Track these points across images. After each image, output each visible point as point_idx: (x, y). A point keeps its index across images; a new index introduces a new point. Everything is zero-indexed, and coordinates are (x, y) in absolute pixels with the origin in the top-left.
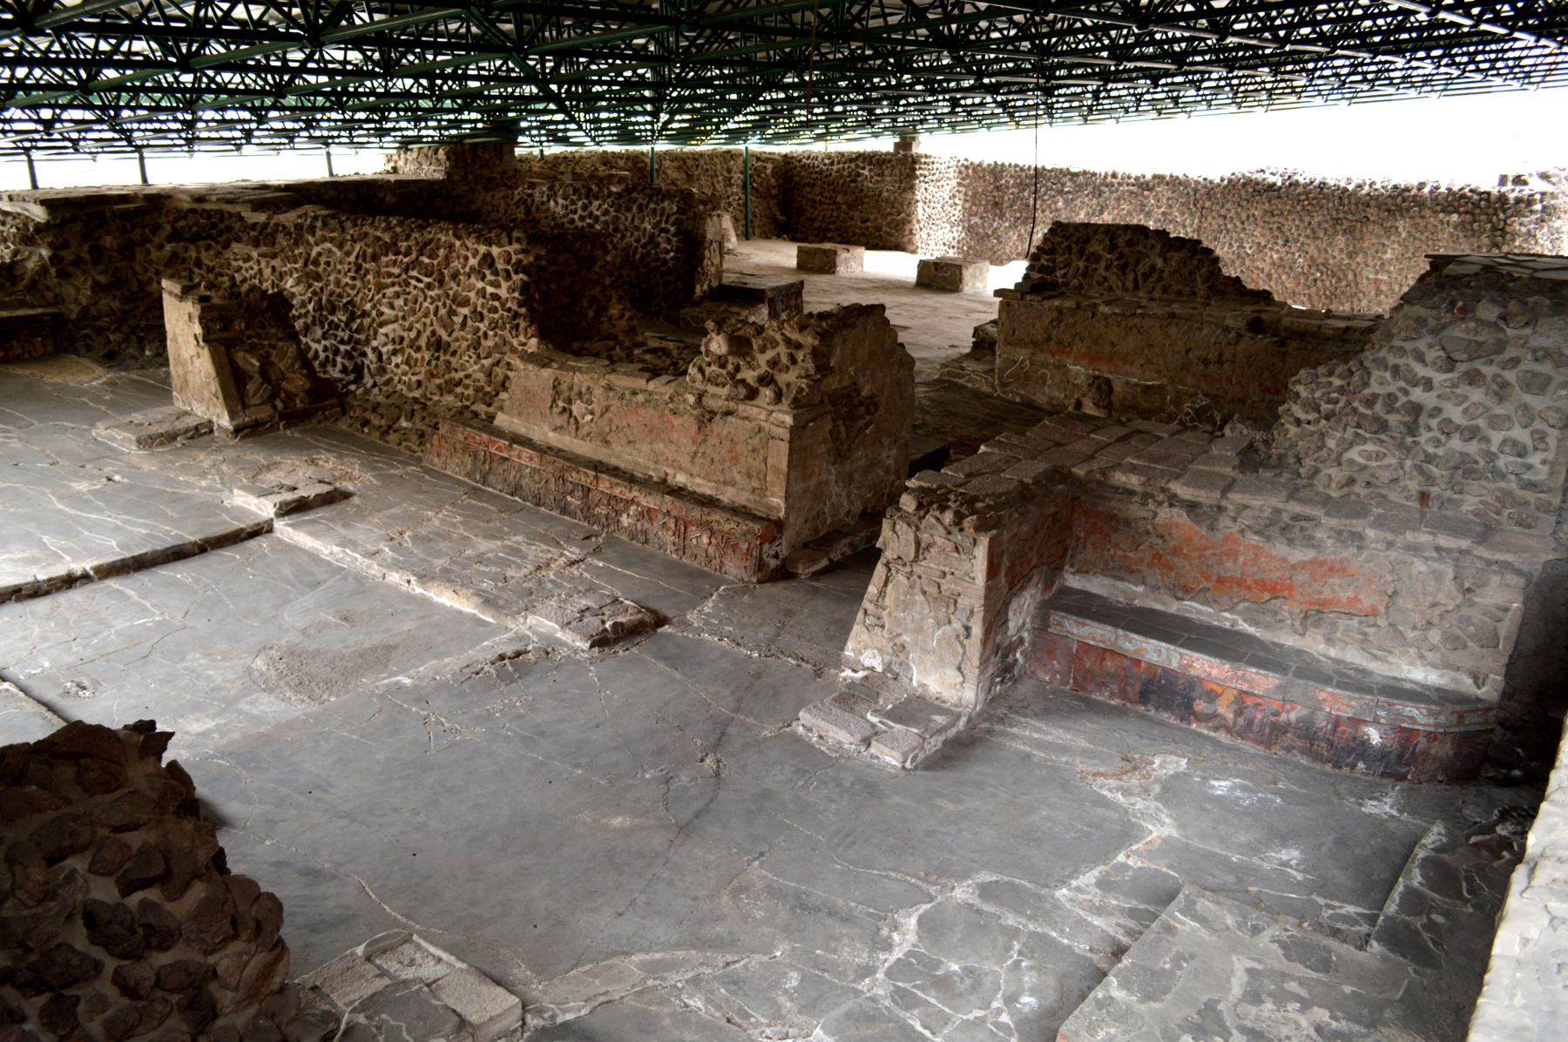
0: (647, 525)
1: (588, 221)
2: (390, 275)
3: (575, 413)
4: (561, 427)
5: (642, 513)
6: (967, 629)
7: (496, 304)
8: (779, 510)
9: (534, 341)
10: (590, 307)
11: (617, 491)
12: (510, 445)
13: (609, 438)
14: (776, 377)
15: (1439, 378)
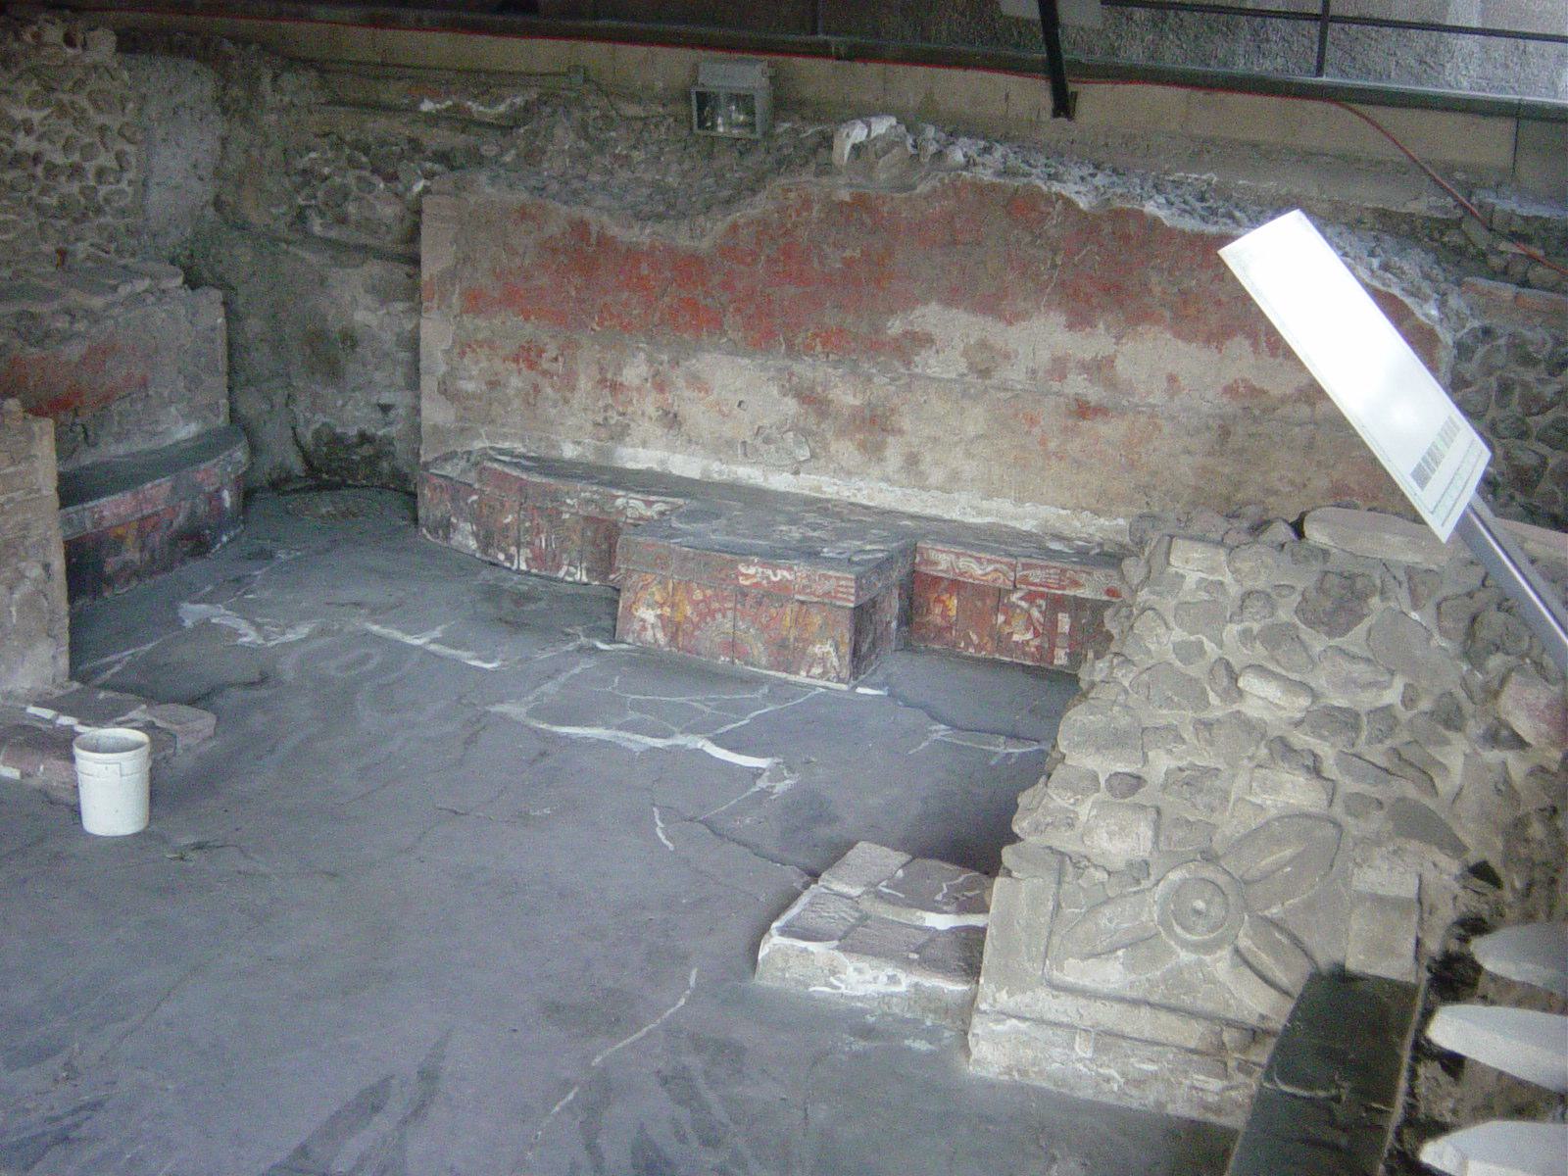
6: (46, 567)
15: (36, 116)
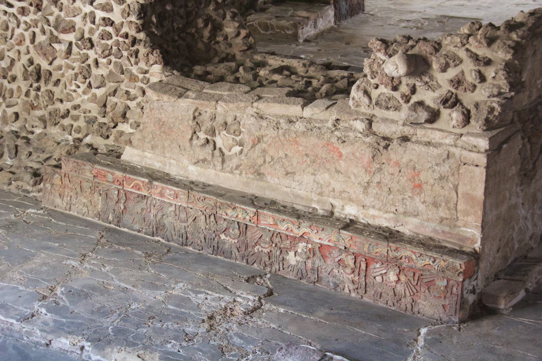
0: (318, 262)
3: (219, 144)
4: (204, 160)
5: (312, 252)
7: (110, 29)
8: (474, 242)
9: (157, 68)
10: (206, 25)
11: (282, 228)
12: (150, 182)
13: (262, 170)
14: (460, 97)
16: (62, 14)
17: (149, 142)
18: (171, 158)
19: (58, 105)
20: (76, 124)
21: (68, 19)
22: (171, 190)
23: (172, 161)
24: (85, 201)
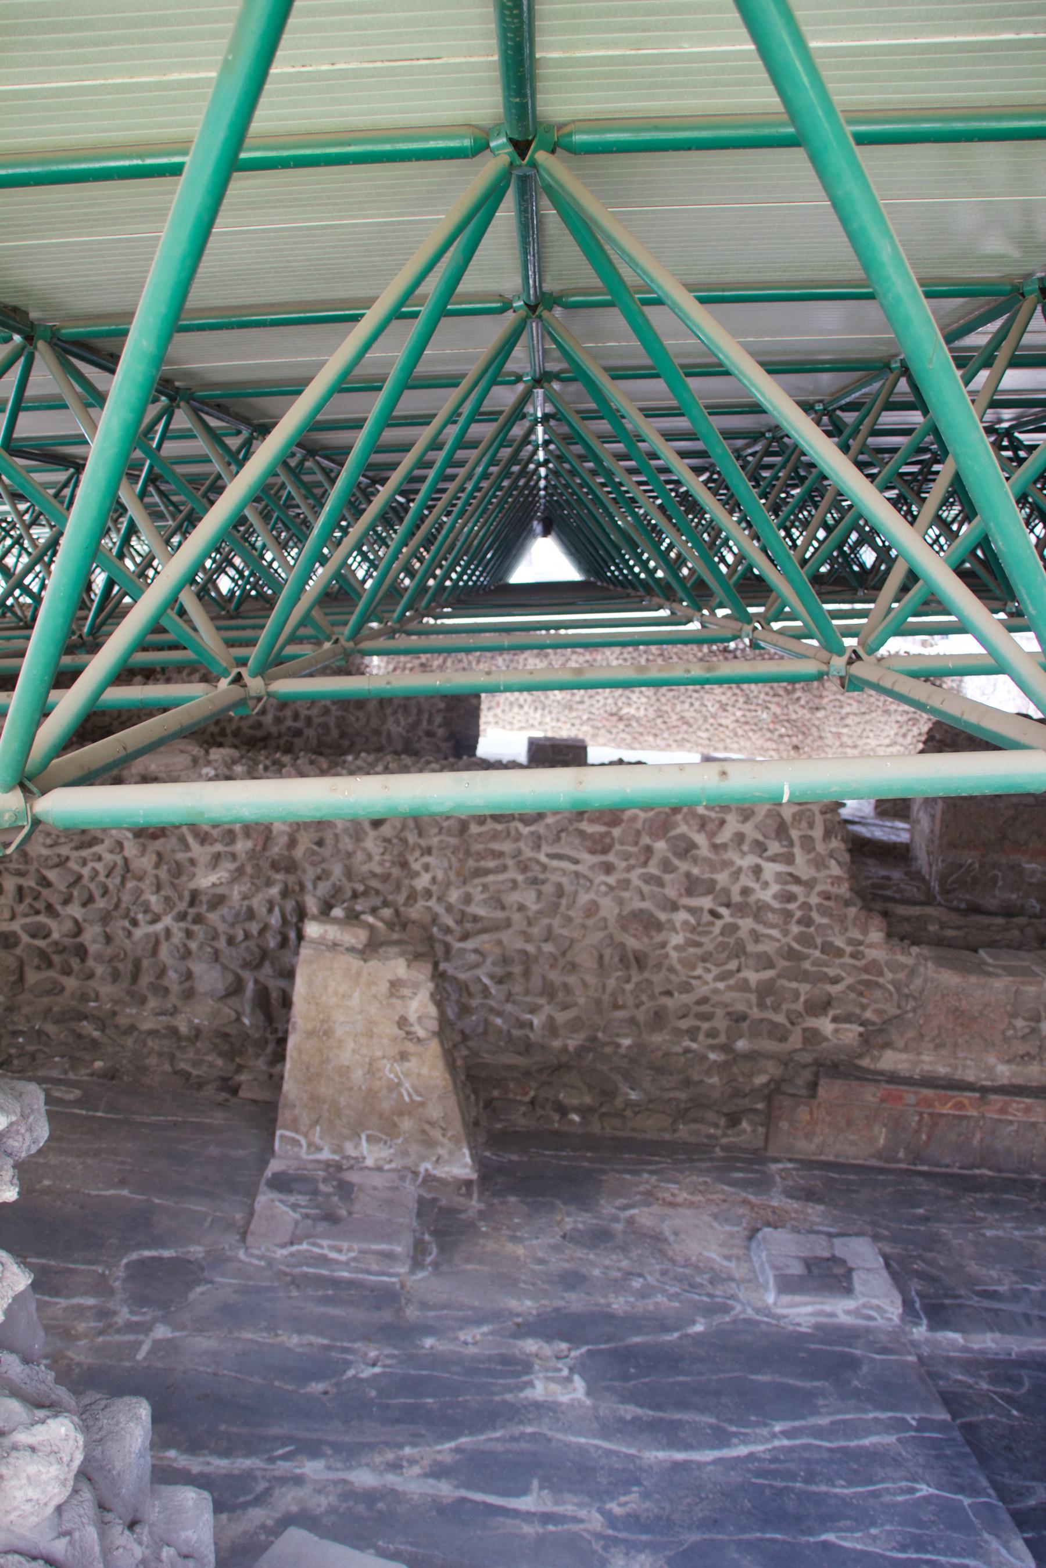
1: (289, 723)
2: (501, 855)
7: (795, 889)
16: (696, 871)
17: (933, 1040)
18: (966, 1058)
19: (666, 1001)
20: (705, 1026)
21: (706, 876)
22: (1018, 1103)
23: (969, 1062)
24: (853, 1137)
